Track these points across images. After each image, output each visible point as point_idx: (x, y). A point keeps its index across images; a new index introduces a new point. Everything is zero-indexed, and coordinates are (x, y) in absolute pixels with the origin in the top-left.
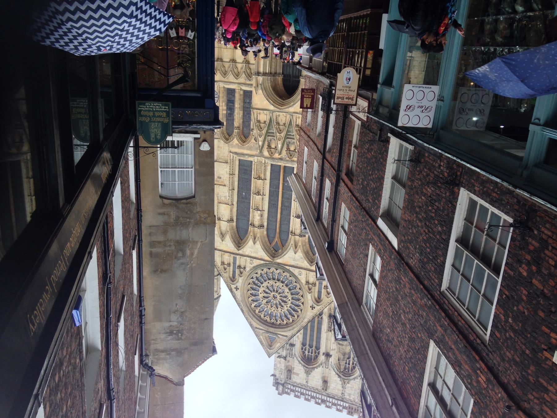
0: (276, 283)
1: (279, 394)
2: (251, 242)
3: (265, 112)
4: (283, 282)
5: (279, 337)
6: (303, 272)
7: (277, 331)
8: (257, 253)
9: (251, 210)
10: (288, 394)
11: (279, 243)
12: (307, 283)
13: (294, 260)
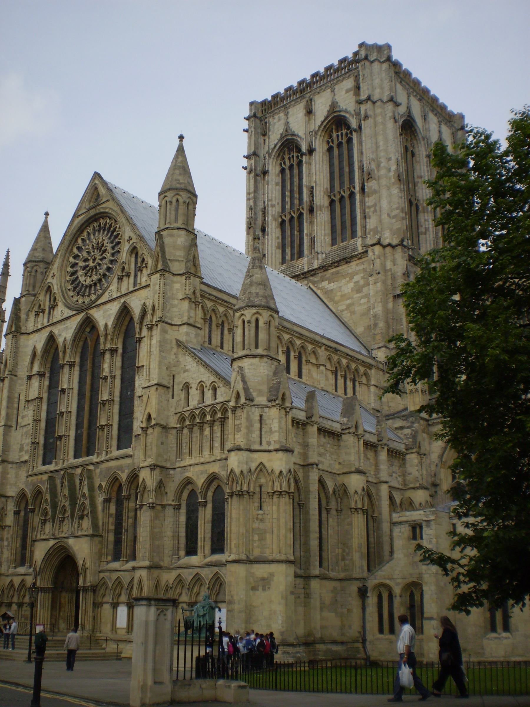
0: (92, 281)
1: (361, 45)
2: (110, 324)
3: (80, 533)
4: (87, 285)
5: (85, 208)
6: (60, 318)
7: (86, 216)
8: (104, 312)
9: (118, 373)
10: (356, 54)
11: (88, 339)
12: (57, 305)
13: (67, 328)
